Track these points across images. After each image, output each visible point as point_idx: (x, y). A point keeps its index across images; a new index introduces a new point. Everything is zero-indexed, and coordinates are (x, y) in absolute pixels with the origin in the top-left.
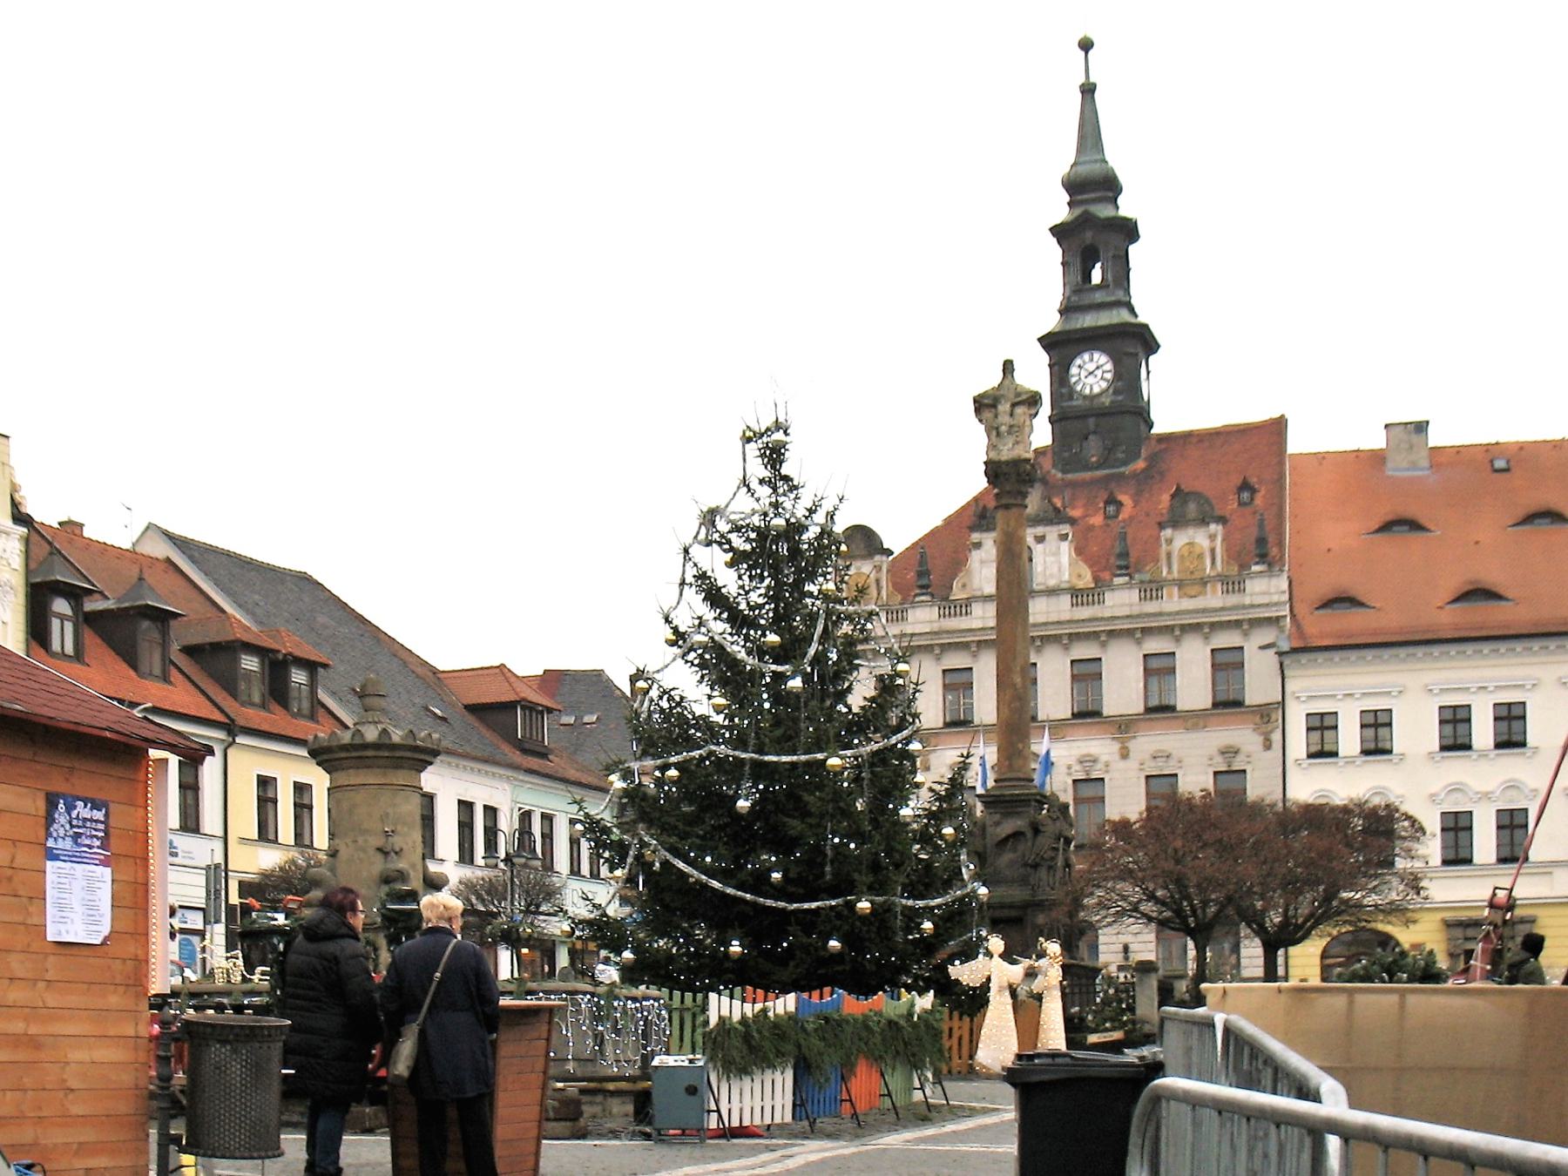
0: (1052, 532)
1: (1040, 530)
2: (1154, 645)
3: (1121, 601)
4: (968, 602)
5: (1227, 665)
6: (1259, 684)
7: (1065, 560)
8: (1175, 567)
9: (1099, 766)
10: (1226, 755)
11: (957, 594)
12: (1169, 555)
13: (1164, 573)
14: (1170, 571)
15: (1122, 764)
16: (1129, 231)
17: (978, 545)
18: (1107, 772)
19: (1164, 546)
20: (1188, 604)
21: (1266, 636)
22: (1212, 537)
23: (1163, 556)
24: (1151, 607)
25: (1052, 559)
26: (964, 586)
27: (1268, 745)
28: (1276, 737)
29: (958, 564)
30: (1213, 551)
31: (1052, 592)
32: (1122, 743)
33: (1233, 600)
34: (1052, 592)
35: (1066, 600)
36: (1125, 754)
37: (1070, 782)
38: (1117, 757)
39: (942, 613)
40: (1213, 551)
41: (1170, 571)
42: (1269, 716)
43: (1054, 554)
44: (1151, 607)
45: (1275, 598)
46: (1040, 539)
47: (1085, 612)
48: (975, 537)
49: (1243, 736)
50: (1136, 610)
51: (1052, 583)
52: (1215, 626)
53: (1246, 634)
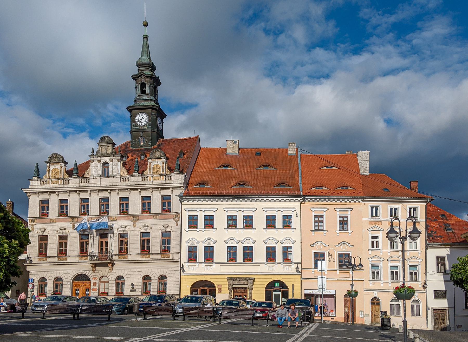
0: (115, 159)
1: (111, 158)
2: (145, 193)
3: (135, 179)
4: (89, 178)
5: (166, 200)
7: (119, 167)
8: (152, 171)
9: (127, 229)
10: (164, 227)
11: (86, 175)
12: (150, 167)
13: (149, 173)
14: (150, 172)
15: (134, 229)
18: (129, 231)
19: (149, 164)
20: (155, 182)
23: (148, 167)
24: (143, 183)
25: (115, 167)
26: (88, 173)
27: (177, 225)
28: (179, 222)
30: (163, 167)
32: (134, 222)
33: (168, 181)
34: (114, 176)
36: (135, 226)
37: (118, 234)
38: (132, 226)
39: (81, 181)
40: (163, 167)
41: (150, 172)
42: (178, 216)
43: (115, 166)
44: (143, 183)
45: (181, 181)
46: (112, 161)
47: (125, 183)
50: (139, 183)
51: (114, 174)
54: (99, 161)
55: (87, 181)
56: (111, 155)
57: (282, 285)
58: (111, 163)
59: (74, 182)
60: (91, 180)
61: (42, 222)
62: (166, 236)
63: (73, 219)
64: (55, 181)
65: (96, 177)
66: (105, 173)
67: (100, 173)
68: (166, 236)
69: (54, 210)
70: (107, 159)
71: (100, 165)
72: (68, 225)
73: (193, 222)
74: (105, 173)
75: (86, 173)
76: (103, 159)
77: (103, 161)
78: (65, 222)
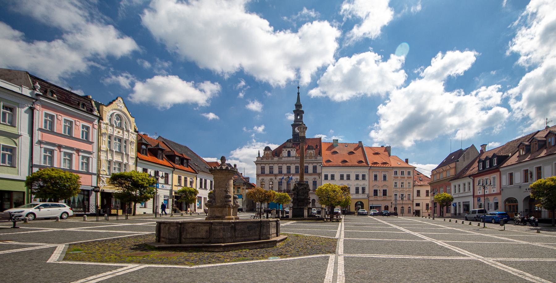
0: (293, 149)
1: (292, 149)
5: (315, 168)
6: (318, 171)
16: (303, 112)
17: (283, 150)
21: (320, 164)
22: (313, 152)
27: (319, 178)
28: (321, 177)
29: (281, 152)
31: (293, 157)
34: (293, 157)
35: (295, 158)
42: (320, 174)
46: (292, 150)
48: (283, 149)
49: (317, 177)
52: (313, 163)
53: (317, 164)
54: (286, 150)
55: (281, 158)
56: (292, 147)
57: (361, 202)
58: (291, 151)
59: (276, 159)
60: (283, 158)
61: (262, 176)
62: (315, 183)
63: (276, 175)
64: (267, 158)
65: (285, 157)
66: (289, 155)
67: (287, 155)
68: (315, 183)
69: (267, 171)
70: (290, 149)
71: (287, 152)
72: (273, 178)
73: (326, 177)
74: (289, 155)
75: (280, 155)
76: (288, 150)
77: (288, 150)
78: (272, 176)
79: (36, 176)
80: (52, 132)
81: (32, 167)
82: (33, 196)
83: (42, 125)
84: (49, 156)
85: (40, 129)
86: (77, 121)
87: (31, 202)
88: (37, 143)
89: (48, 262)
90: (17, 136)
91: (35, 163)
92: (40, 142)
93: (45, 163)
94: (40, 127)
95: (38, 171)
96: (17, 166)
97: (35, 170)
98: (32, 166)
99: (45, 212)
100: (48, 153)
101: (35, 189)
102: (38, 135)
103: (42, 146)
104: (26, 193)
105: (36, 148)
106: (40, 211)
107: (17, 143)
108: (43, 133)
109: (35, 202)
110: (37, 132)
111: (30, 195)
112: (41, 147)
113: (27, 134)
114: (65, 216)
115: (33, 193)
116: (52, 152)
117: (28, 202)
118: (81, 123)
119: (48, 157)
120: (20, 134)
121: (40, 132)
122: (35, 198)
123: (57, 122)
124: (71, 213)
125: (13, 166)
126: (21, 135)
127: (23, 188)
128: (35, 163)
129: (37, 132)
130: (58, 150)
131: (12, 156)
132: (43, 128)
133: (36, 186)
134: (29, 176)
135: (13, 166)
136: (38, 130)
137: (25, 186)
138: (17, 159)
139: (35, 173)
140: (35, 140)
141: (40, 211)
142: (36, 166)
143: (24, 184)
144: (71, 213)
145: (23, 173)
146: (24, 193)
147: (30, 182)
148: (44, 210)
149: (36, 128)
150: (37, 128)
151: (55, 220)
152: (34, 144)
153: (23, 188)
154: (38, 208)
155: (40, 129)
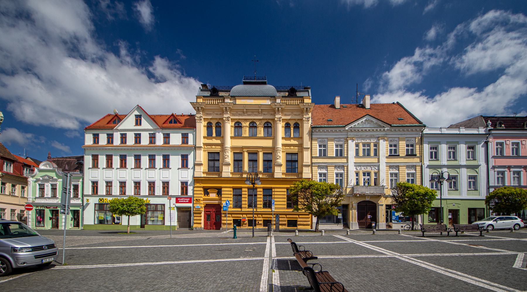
79: (493, 195)
80: (502, 156)
81: (489, 188)
82: (491, 211)
83: (494, 153)
84: (501, 177)
85: (494, 157)
86: (523, 141)
87: (489, 216)
88: (491, 169)
89: (514, 267)
90: (477, 167)
91: (490, 185)
92: (494, 167)
93: (498, 182)
94: (493, 155)
95: (494, 191)
96: (478, 189)
97: (492, 190)
98: (489, 187)
99: (500, 224)
100: (500, 174)
101: (493, 206)
102: (492, 162)
103: (496, 170)
104: (485, 209)
105: (491, 172)
106: (497, 223)
107: (478, 172)
108: (496, 160)
109: (492, 216)
110: (491, 159)
111: (488, 210)
112: (494, 171)
113: (484, 163)
114: (517, 228)
115: (490, 208)
116: (503, 173)
117: (487, 217)
118: (510, 142)
119: (500, 178)
120: (479, 164)
121: (493, 159)
122: (492, 212)
123: (506, 148)
124: (522, 224)
125: (476, 189)
126: (480, 165)
127: (483, 205)
128: (490, 185)
129: (491, 159)
130: (508, 171)
131: (475, 182)
132: (495, 155)
133: (493, 203)
134: (487, 195)
135: (476, 189)
136: (491, 158)
137: (485, 204)
138: (478, 184)
139: (491, 193)
140: (490, 166)
141: (497, 223)
142: (492, 187)
143: (484, 202)
144: (522, 224)
145: (483, 194)
146: (484, 209)
147: (488, 200)
148: (499, 222)
149: (490, 156)
150: (491, 157)
151: (510, 231)
152: (489, 170)
153: (483, 205)
154: (496, 220)
155: (494, 157)
